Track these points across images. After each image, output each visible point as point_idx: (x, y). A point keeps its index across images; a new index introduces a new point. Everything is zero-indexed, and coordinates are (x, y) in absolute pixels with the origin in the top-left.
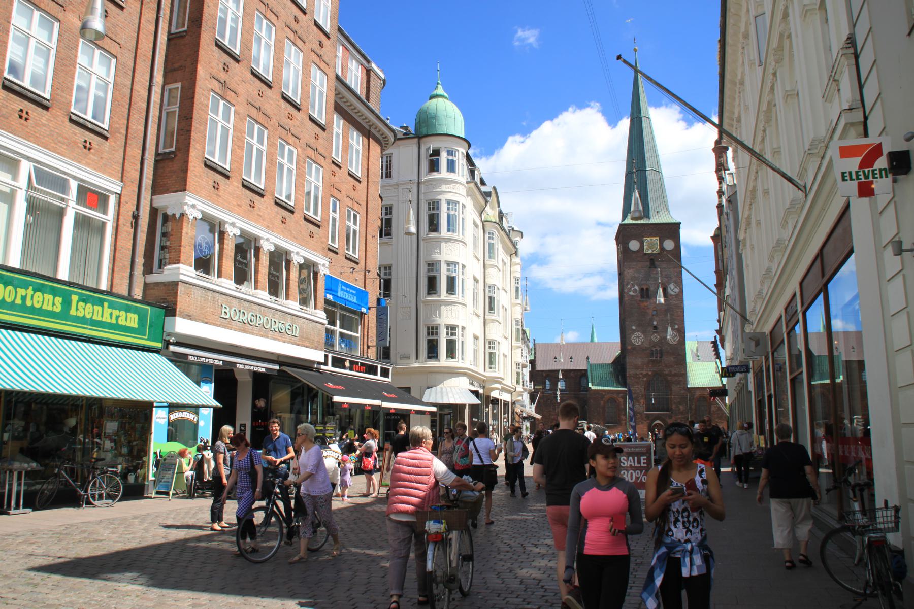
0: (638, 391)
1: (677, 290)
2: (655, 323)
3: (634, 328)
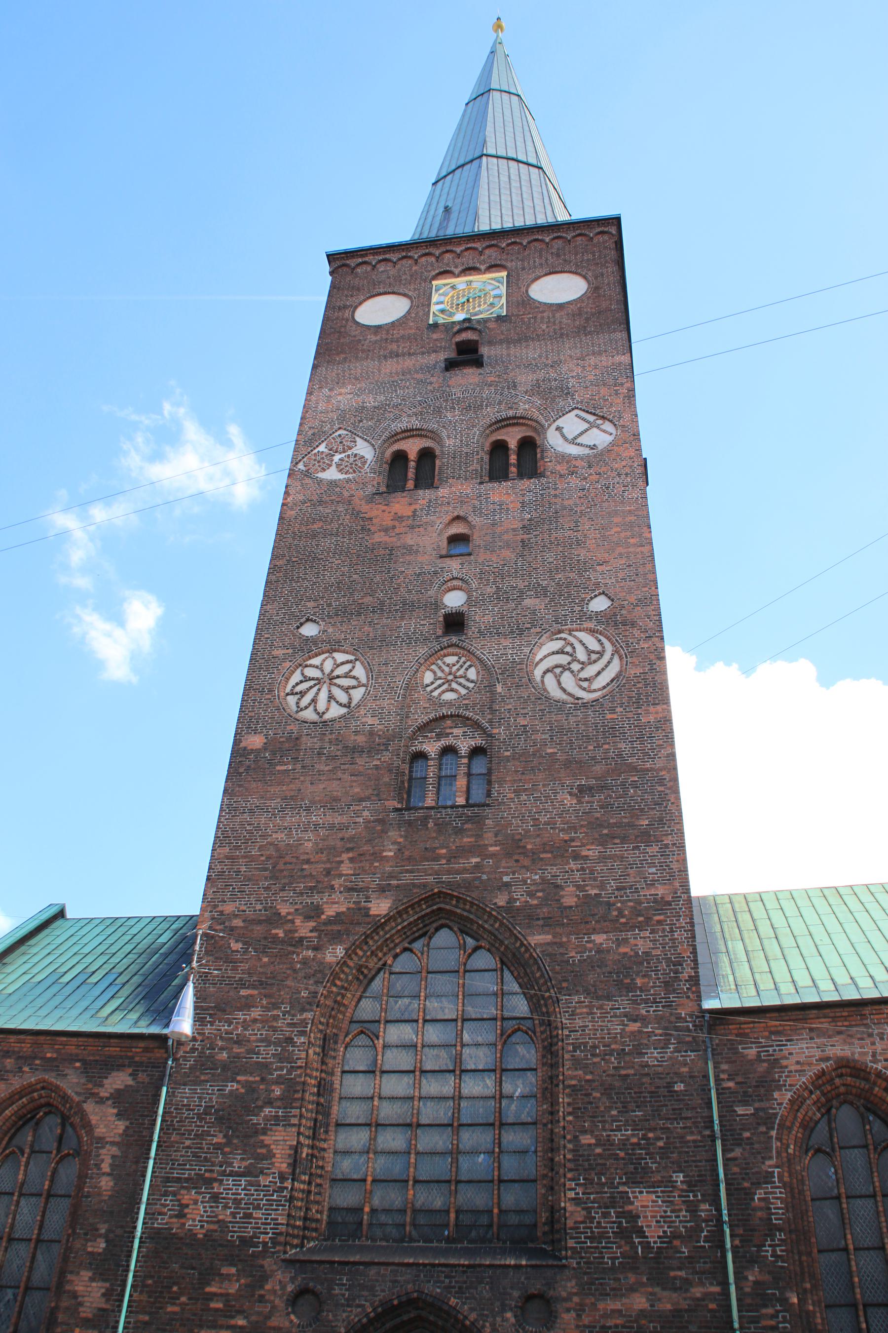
0: (267, 1053)
3: (309, 630)
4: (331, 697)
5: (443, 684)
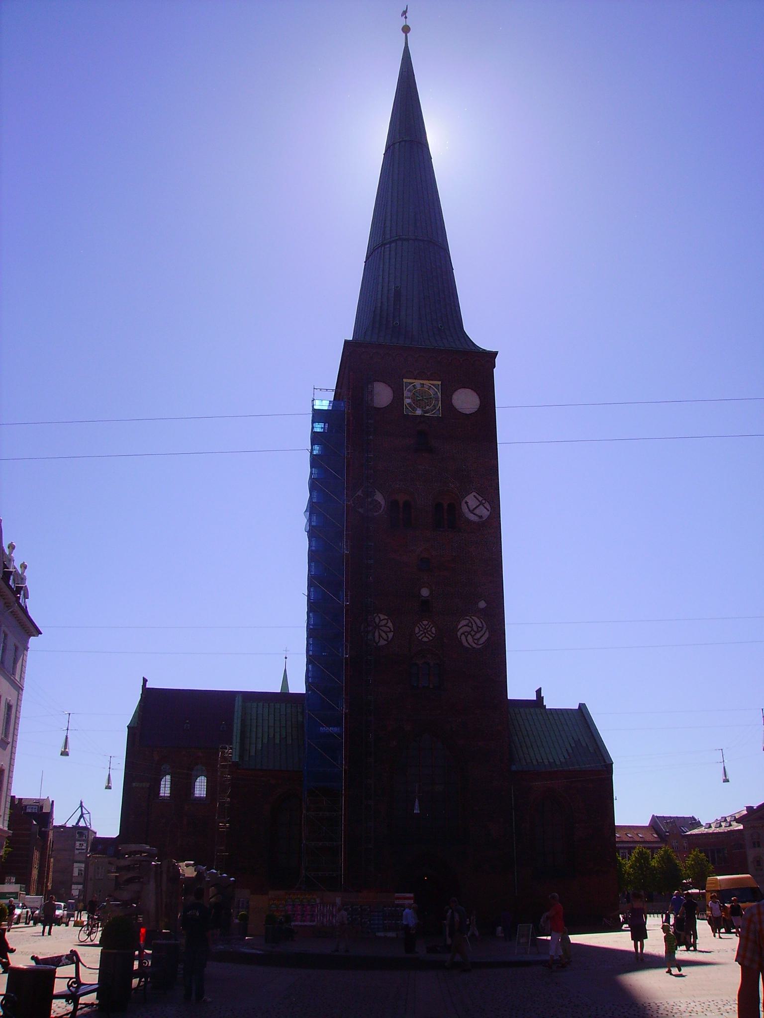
1: (484, 512)
2: (425, 592)
4: (380, 636)
5: (423, 634)
